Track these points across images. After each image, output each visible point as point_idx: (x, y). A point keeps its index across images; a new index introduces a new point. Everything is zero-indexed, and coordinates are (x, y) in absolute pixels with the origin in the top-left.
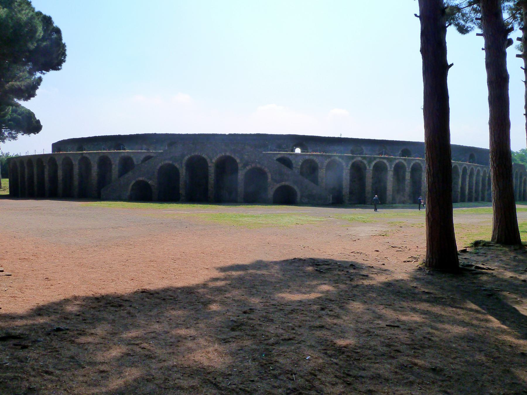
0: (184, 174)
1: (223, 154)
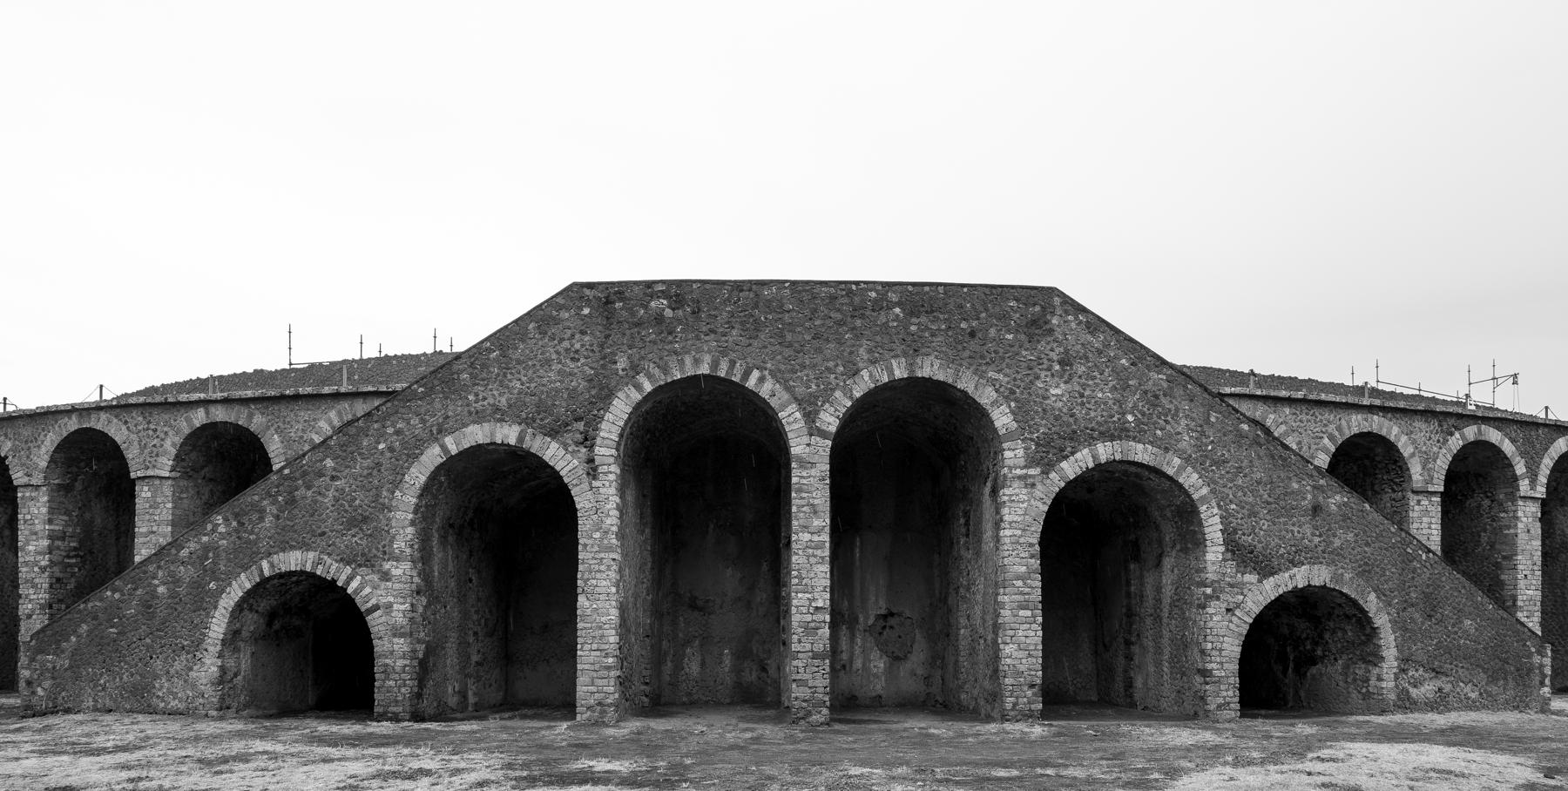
0: (612, 521)
1: (900, 373)
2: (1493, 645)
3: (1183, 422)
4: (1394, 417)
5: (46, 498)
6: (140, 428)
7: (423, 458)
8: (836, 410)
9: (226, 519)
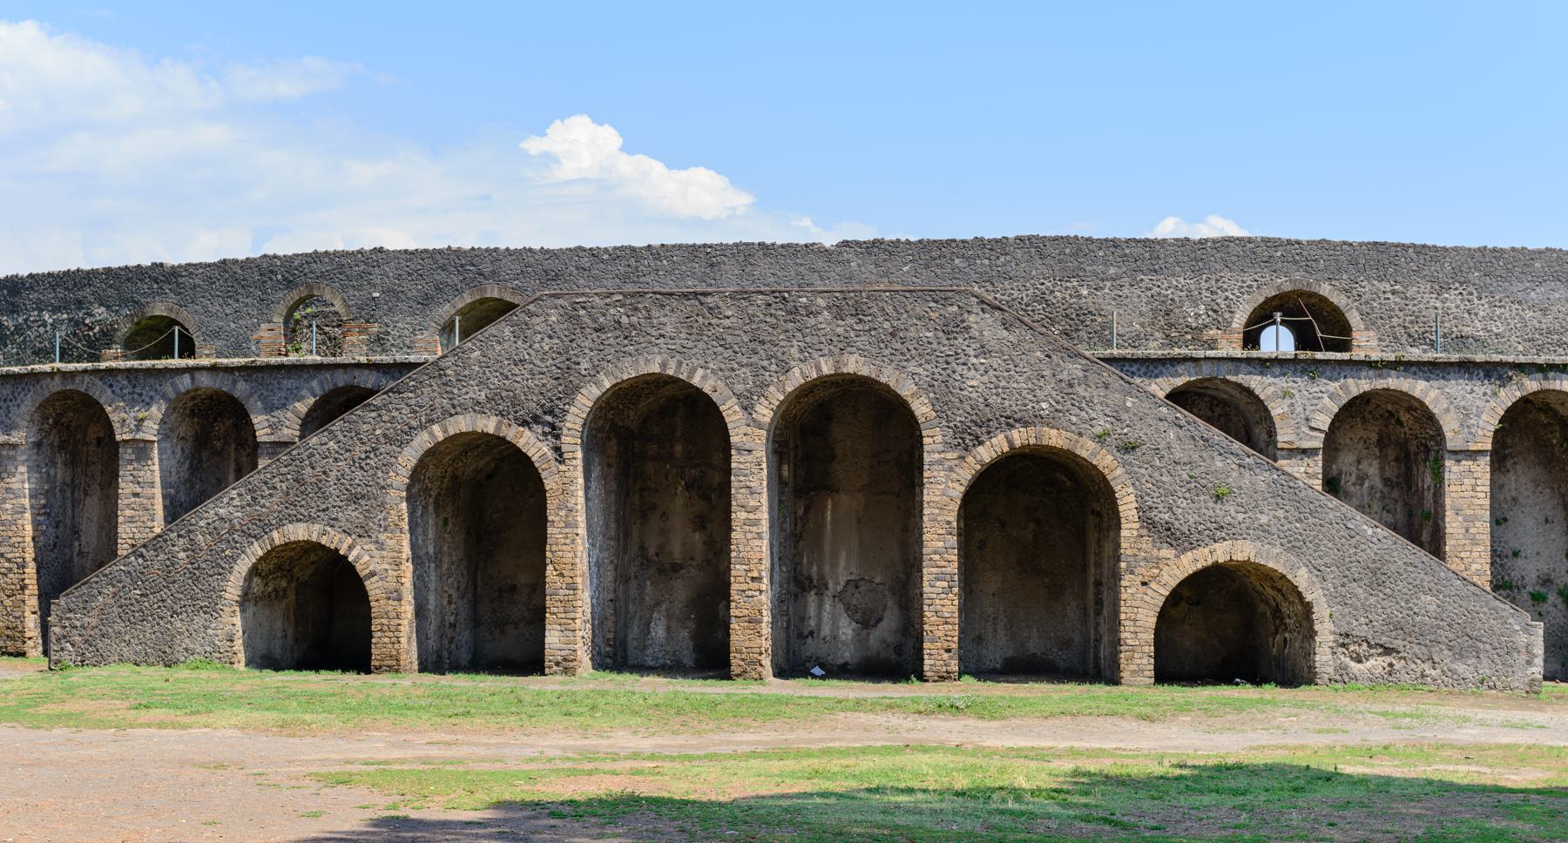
1: (827, 369)
2: (1460, 621)
3: (1099, 407)
4: (1420, 370)
6: (126, 391)
7: (414, 443)
8: (770, 403)
9: (240, 495)
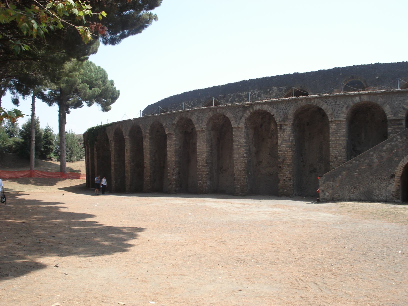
5: (290, 129)
